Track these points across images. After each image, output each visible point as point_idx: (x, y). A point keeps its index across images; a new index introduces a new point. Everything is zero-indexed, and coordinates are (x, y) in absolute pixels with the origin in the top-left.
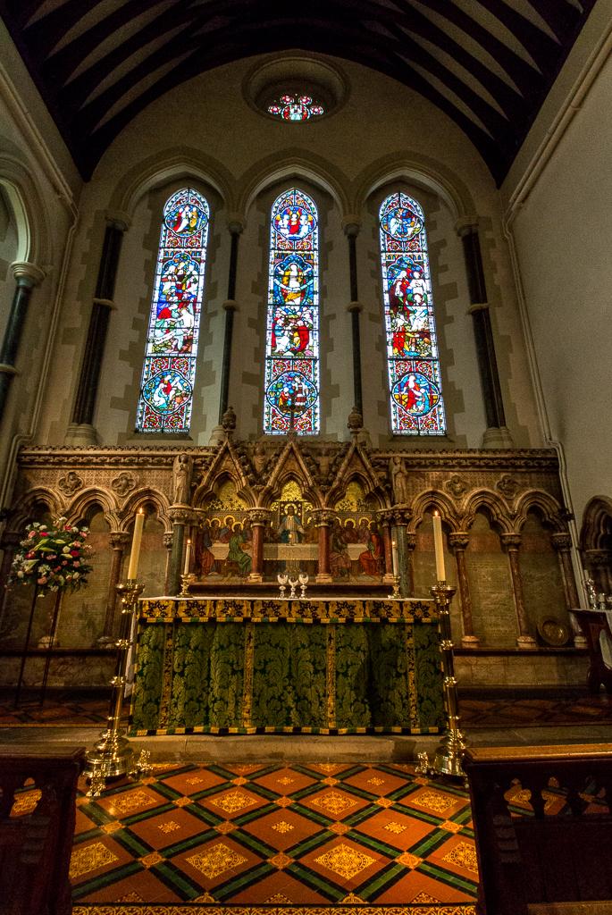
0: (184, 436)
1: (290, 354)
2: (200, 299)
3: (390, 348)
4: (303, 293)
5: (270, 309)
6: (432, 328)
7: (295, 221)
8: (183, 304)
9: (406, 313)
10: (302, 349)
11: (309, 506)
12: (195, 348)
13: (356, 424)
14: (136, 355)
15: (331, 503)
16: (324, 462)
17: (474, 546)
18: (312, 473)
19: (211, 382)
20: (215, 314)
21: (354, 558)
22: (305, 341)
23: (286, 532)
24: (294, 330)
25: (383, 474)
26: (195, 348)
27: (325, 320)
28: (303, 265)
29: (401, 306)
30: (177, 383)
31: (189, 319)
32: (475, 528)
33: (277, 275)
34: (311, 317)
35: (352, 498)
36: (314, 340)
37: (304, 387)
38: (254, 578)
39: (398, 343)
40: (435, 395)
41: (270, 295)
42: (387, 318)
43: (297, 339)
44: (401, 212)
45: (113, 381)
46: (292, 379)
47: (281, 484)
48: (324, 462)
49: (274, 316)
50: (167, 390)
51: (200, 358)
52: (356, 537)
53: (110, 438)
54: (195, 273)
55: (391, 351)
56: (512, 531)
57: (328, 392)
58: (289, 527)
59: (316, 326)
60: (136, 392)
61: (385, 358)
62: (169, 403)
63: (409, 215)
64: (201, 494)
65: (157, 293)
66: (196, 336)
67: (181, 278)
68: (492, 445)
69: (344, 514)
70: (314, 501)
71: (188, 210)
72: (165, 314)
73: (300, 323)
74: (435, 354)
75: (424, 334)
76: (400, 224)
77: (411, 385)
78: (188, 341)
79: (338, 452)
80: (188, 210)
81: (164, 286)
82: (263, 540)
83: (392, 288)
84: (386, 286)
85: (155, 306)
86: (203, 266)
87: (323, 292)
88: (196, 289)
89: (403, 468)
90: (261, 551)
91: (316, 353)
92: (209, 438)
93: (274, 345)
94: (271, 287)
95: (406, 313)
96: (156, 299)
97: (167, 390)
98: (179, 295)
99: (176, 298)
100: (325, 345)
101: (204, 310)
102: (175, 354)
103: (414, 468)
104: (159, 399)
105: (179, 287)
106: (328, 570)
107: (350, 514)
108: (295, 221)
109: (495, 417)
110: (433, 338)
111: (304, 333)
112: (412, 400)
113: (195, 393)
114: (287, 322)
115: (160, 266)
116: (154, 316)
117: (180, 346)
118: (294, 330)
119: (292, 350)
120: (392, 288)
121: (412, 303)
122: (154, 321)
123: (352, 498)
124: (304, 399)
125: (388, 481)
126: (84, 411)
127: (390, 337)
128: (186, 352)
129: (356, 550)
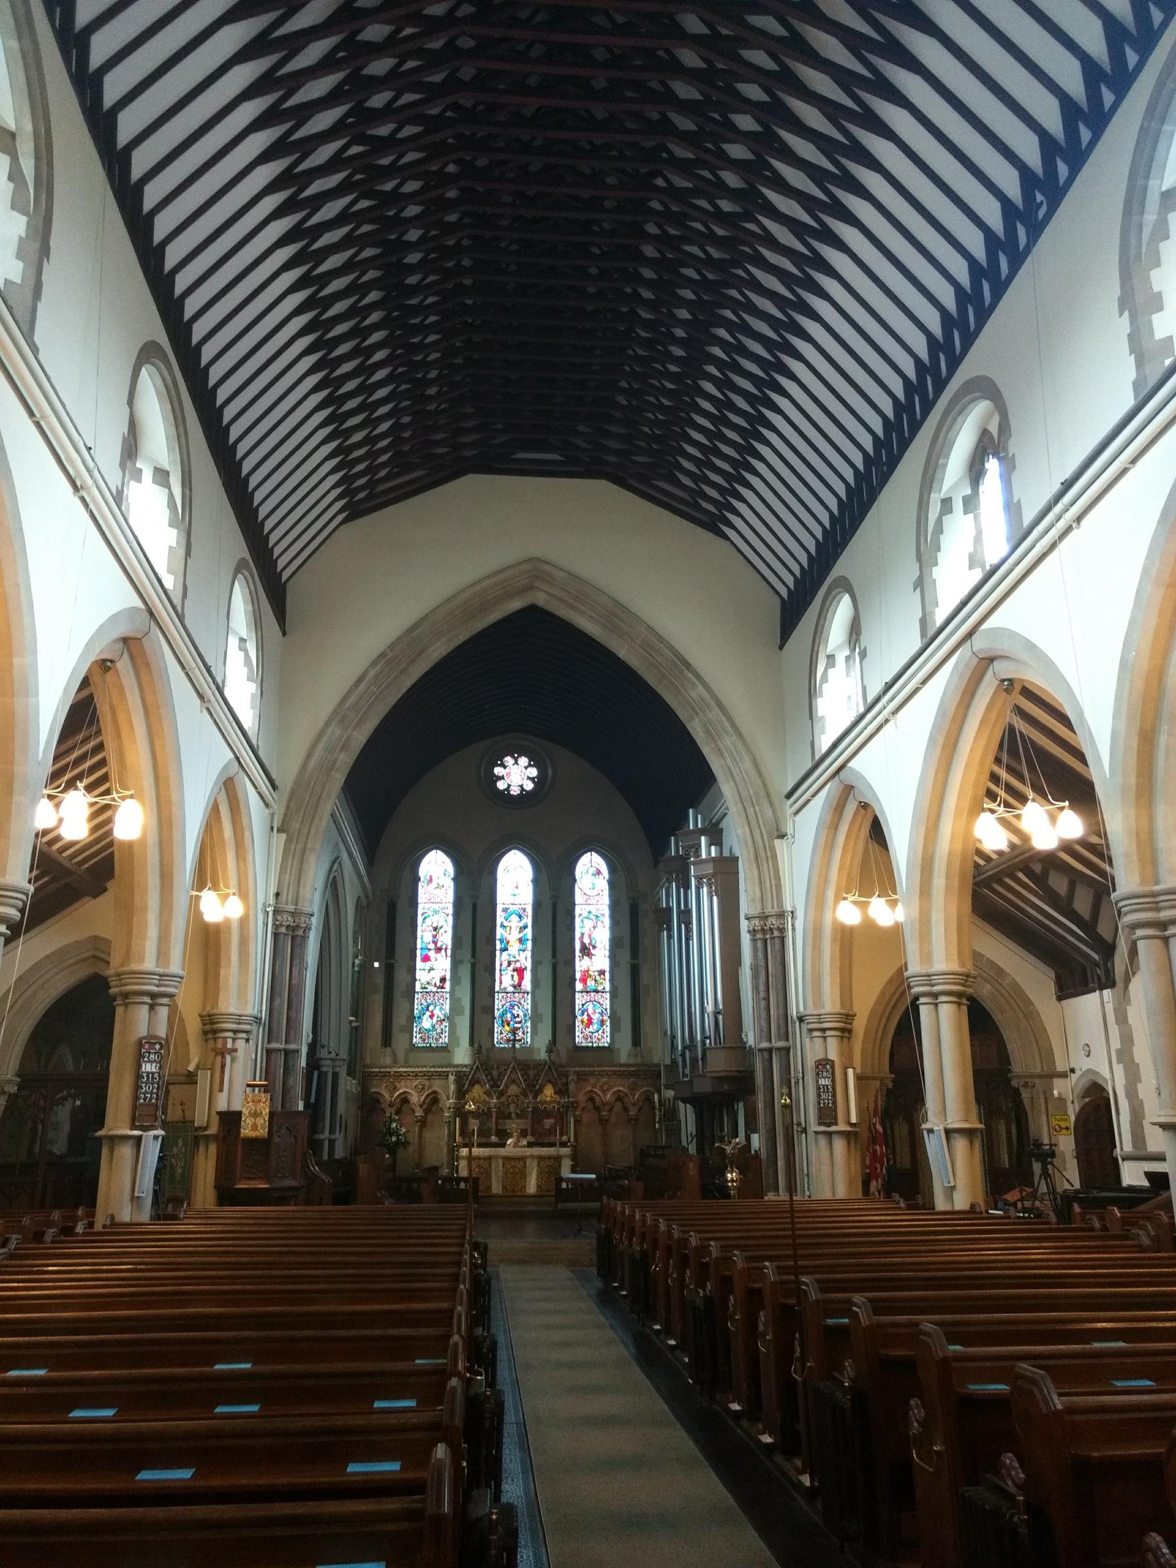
0: (444, 1049)
1: (511, 989)
2: (450, 947)
3: (577, 983)
4: (521, 941)
5: (498, 953)
6: (607, 969)
7: (515, 877)
8: (438, 950)
9: (589, 955)
10: (519, 985)
11: (522, 1098)
12: (448, 985)
13: (552, 1047)
14: (410, 992)
15: (535, 1097)
16: (532, 1073)
17: (613, 1119)
18: (525, 1081)
19: (462, 1013)
20: (462, 962)
21: (547, 1127)
22: (521, 977)
23: (510, 1113)
24: (514, 970)
25: (564, 1080)
26: (448, 985)
27: (536, 963)
28: (520, 917)
29: (586, 951)
30: (437, 1012)
31: (442, 965)
32: (615, 1110)
33: (502, 926)
34: (525, 960)
35: (549, 1091)
36: (528, 975)
37: (521, 1014)
38: (494, 1138)
39: (584, 981)
40: (605, 1018)
41: (498, 943)
42: (577, 959)
43: (516, 977)
44: (593, 870)
45: (399, 1020)
46: (512, 1007)
47: (507, 1086)
48: (532, 1073)
49: (501, 959)
50: (432, 1017)
51: (452, 993)
52: (549, 1115)
53: (401, 1058)
54: (445, 924)
55: (579, 986)
56: (633, 1112)
57: (535, 1017)
58: (512, 1110)
59: (529, 968)
60: (411, 1018)
61: (574, 992)
62: (433, 1026)
63: (599, 873)
64: (461, 1094)
65: (419, 941)
66: (448, 977)
67: (435, 929)
68: (632, 1061)
69: (542, 1102)
70: (526, 1096)
71: (436, 871)
72: (426, 959)
73: (518, 965)
74: (608, 989)
75: (602, 973)
76: (592, 877)
77: (590, 1011)
78: (443, 980)
79: (539, 1066)
80: (436, 871)
81: (424, 936)
82: (498, 1118)
83: (583, 934)
84: (577, 935)
85: (418, 952)
86: (450, 919)
87: (534, 940)
88: (446, 939)
89: (575, 1078)
90: (497, 1123)
91: (529, 989)
92: (462, 1056)
93: (501, 983)
94: (498, 936)
95: (589, 955)
96: (419, 946)
97: (432, 1017)
98: (435, 943)
99: (432, 946)
100: (535, 981)
101: (453, 956)
102: (435, 989)
103: (582, 1077)
104: (426, 1023)
105: (435, 936)
106: (533, 1134)
107: (546, 1102)
108: (515, 877)
109: (636, 1041)
110: (607, 975)
111: (520, 972)
112: (590, 1022)
113: (450, 1018)
114: (509, 964)
115: (420, 919)
116: (418, 959)
117: (438, 984)
118: (514, 970)
119: (514, 987)
120: (583, 934)
121: (594, 947)
122: (419, 964)
123: (549, 1091)
124: (520, 1022)
125: (566, 1084)
126: (387, 1041)
127: (578, 975)
128: (442, 988)
129: (548, 1123)
